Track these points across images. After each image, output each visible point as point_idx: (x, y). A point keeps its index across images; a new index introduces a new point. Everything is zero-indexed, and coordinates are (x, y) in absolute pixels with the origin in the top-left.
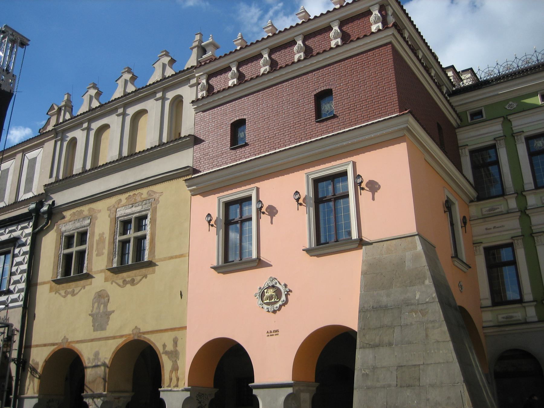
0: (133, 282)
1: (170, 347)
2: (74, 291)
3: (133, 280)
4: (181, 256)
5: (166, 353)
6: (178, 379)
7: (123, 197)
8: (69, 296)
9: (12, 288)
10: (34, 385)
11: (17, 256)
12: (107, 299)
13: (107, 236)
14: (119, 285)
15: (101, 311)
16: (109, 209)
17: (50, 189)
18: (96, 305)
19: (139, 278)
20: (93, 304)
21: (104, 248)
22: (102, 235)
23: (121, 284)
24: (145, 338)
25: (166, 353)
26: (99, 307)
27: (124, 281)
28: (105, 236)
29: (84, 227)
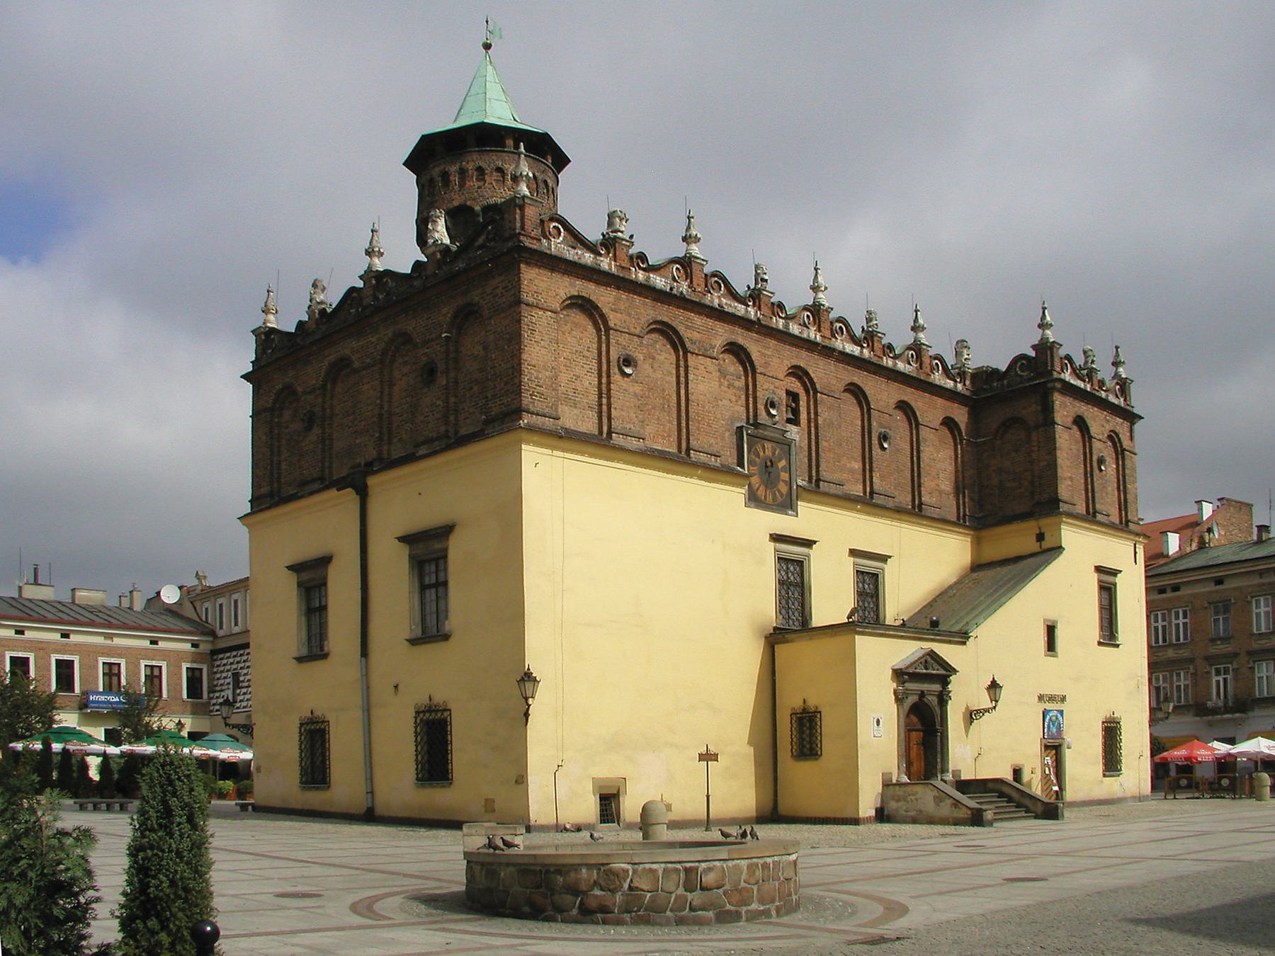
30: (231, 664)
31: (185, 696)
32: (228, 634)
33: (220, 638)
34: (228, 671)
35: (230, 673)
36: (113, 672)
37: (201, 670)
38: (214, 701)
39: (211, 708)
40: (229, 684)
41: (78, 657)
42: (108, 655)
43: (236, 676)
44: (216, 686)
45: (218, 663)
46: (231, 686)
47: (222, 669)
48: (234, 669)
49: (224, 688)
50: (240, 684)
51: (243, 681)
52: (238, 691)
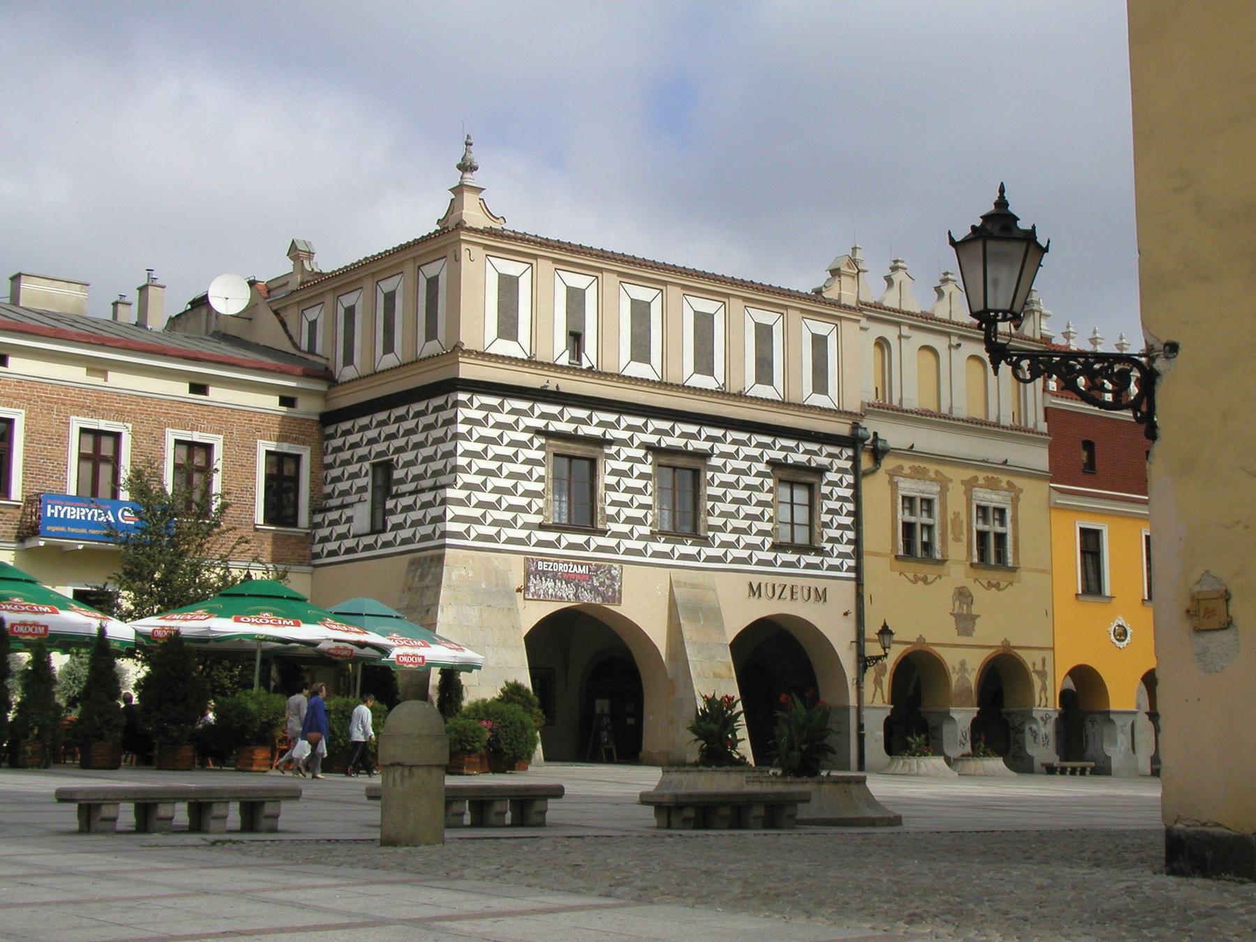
0: (997, 586)
1: (1039, 667)
2: (927, 579)
3: (998, 584)
4: (1043, 571)
5: (1036, 672)
6: (1047, 699)
7: (981, 475)
8: (920, 583)
9: (828, 546)
10: (882, 692)
11: (826, 497)
12: (970, 599)
13: (963, 517)
14: (984, 587)
15: (965, 612)
16: (963, 482)
17: (870, 410)
18: (957, 603)
19: (1006, 584)
20: (954, 601)
21: (962, 533)
22: (957, 515)
23: (986, 585)
24: (1016, 653)
25: (1036, 672)
26: (961, 607)
27: (989, 582)
28: (961, 517)
29: (932, 494)
30: (372, 441)
31: (259, 517)
32: (368, 372)
33: (342, 383)
34: (362, 459)
35: (367, 465)
36: (103, 453)
37: (297, 458)
38: (324, 532)
39: (317, 548)
40: (362, 489)
41: (23, 411)
42: (94, 412)
43: (384, 469)
44: (330, 496)
45: (337, 442)
46: (368, 496)
47: (346, 455)
48: (379, 454)
49: (348, 500)
50: (394, 489)
51: (402, 481)
52: (390, 504)
